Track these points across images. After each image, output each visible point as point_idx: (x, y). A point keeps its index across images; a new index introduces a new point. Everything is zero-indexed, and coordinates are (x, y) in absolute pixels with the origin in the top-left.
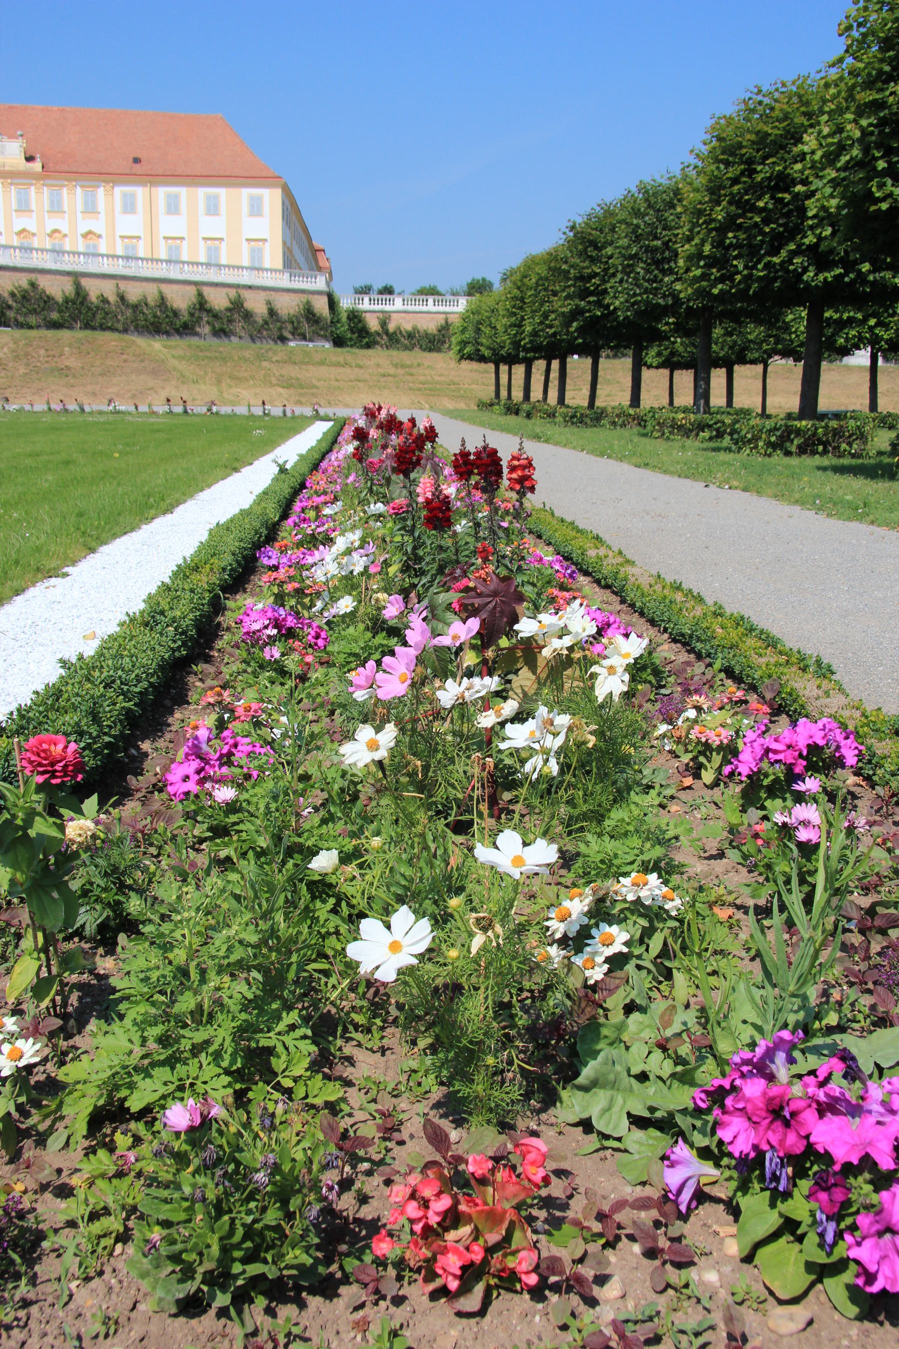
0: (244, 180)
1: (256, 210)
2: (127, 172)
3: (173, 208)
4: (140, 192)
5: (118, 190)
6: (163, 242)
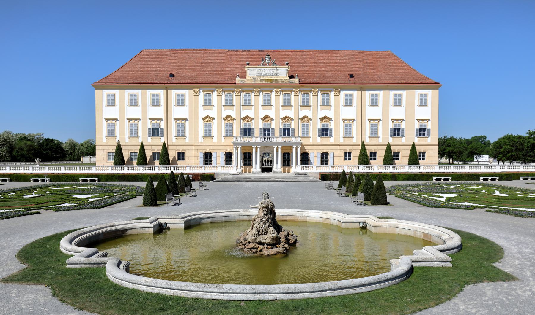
0: (421, 85)
1: (423, 102)
3: (374, 102)
6: (368, 122)
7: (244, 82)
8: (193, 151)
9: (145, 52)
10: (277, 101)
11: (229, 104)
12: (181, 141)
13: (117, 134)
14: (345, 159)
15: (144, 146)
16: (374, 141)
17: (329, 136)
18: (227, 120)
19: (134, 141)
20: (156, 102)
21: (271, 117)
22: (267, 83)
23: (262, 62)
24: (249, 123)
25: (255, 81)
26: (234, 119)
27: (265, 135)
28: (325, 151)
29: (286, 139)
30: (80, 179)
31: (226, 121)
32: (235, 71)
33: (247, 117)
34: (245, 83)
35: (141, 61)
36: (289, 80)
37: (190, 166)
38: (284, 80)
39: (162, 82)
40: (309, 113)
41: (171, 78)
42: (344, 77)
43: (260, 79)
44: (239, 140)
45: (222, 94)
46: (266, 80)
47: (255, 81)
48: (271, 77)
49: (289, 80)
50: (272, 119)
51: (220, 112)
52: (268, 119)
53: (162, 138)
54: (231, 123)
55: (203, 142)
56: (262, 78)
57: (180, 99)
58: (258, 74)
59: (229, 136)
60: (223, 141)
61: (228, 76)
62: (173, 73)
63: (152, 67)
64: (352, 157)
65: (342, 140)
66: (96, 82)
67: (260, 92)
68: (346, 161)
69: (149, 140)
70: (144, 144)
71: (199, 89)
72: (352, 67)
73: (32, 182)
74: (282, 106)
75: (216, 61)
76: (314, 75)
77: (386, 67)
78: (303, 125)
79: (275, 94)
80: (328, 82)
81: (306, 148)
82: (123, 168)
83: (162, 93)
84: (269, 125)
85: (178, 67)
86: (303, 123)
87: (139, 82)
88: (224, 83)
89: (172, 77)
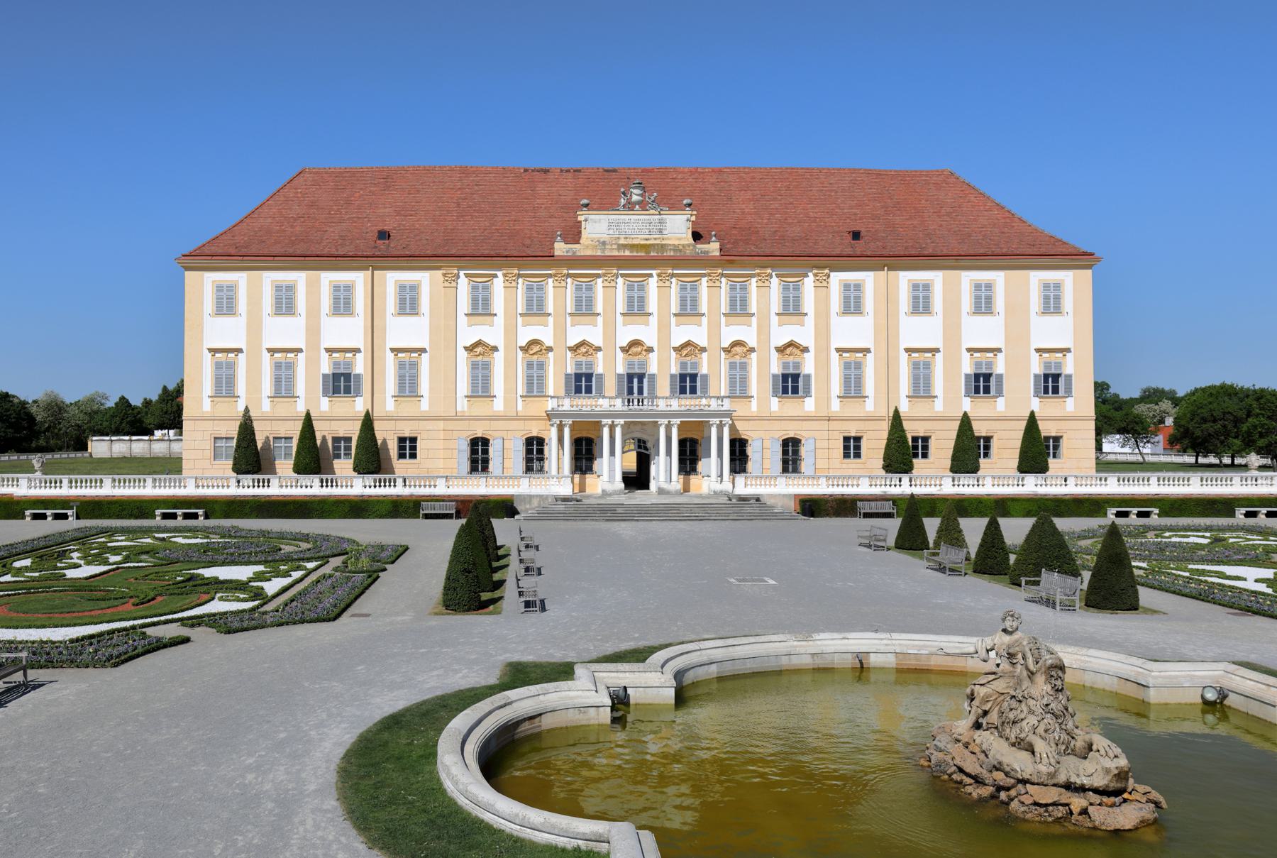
2: (848, 251)
4: (868, 279)
5: (838, 279)
6: (904, 356)
7: (574, 253)
8: (441, 435)
9: (307, 175)
10: (663, 300)
11: (535, 309)
12: (408, 408)
13: (241, 387)
14: (846, 455)
15: (311, 422)
16: (922, 408)
17: (801, 393)
18: (531, 352)
19: (284, 408)
20: (342, 305)
21: (648, 343)
22: (635, 254)
23: (622, 200)
24: (590, 359)
25: (603, 250)
26: (550, 349)
27: (630, 392)
28: (791, 435)
29: (692, 403)
30: (158, 512)
31: (527, 355)
32: (547, 224)
33: (583, 343)
34: (578, 254)
35: (298, 198)
36: (695, 247)
37: (447, 477)
38: (681, 247)
39: (360, 254)
40: (748, 335)
41: (382, 242)
42: (838, 239)
43: (619, 245)
44: (567, 405)
45: (518, 283)
46: (632, 247)
47: (603, 250)
48: (647, 240)
49: (693, 245)
50: (650, 350)
51: (511, 331)
52: (639, 349)
53: (356, 399)
54: (542, 359)
55: (466, 409)
56: (622, 242)
57: (408, 296)
58: (611, 232)
59: (535, 394)
60: (520, 408)
61: (530, 238)
62: (386, 228)
63: (329, 213)
64: (863, 451)
65: (836, 406)
66: (186, 253)
67: (617, 278)
68: (847, 460)
69: (324, 405)
70: (312, 415)
71: (456, 272)
72: (854, 211)
73: (28, 519)
74: (675, 315)
75: (496, 197)
76: (757, 233)
77: (943, 212)
78: (732, 366)
79: (656, 285)
80: (798, 253)
81: (740, 426)
82: (269, 482)
83: (358, 279)
84: (643, 365)
85: (398, 214)
86: (732, 360)
87: (298, 252)
88: (524, 254)
89: (385, 239)
